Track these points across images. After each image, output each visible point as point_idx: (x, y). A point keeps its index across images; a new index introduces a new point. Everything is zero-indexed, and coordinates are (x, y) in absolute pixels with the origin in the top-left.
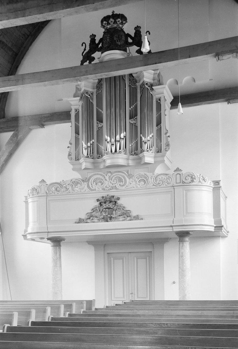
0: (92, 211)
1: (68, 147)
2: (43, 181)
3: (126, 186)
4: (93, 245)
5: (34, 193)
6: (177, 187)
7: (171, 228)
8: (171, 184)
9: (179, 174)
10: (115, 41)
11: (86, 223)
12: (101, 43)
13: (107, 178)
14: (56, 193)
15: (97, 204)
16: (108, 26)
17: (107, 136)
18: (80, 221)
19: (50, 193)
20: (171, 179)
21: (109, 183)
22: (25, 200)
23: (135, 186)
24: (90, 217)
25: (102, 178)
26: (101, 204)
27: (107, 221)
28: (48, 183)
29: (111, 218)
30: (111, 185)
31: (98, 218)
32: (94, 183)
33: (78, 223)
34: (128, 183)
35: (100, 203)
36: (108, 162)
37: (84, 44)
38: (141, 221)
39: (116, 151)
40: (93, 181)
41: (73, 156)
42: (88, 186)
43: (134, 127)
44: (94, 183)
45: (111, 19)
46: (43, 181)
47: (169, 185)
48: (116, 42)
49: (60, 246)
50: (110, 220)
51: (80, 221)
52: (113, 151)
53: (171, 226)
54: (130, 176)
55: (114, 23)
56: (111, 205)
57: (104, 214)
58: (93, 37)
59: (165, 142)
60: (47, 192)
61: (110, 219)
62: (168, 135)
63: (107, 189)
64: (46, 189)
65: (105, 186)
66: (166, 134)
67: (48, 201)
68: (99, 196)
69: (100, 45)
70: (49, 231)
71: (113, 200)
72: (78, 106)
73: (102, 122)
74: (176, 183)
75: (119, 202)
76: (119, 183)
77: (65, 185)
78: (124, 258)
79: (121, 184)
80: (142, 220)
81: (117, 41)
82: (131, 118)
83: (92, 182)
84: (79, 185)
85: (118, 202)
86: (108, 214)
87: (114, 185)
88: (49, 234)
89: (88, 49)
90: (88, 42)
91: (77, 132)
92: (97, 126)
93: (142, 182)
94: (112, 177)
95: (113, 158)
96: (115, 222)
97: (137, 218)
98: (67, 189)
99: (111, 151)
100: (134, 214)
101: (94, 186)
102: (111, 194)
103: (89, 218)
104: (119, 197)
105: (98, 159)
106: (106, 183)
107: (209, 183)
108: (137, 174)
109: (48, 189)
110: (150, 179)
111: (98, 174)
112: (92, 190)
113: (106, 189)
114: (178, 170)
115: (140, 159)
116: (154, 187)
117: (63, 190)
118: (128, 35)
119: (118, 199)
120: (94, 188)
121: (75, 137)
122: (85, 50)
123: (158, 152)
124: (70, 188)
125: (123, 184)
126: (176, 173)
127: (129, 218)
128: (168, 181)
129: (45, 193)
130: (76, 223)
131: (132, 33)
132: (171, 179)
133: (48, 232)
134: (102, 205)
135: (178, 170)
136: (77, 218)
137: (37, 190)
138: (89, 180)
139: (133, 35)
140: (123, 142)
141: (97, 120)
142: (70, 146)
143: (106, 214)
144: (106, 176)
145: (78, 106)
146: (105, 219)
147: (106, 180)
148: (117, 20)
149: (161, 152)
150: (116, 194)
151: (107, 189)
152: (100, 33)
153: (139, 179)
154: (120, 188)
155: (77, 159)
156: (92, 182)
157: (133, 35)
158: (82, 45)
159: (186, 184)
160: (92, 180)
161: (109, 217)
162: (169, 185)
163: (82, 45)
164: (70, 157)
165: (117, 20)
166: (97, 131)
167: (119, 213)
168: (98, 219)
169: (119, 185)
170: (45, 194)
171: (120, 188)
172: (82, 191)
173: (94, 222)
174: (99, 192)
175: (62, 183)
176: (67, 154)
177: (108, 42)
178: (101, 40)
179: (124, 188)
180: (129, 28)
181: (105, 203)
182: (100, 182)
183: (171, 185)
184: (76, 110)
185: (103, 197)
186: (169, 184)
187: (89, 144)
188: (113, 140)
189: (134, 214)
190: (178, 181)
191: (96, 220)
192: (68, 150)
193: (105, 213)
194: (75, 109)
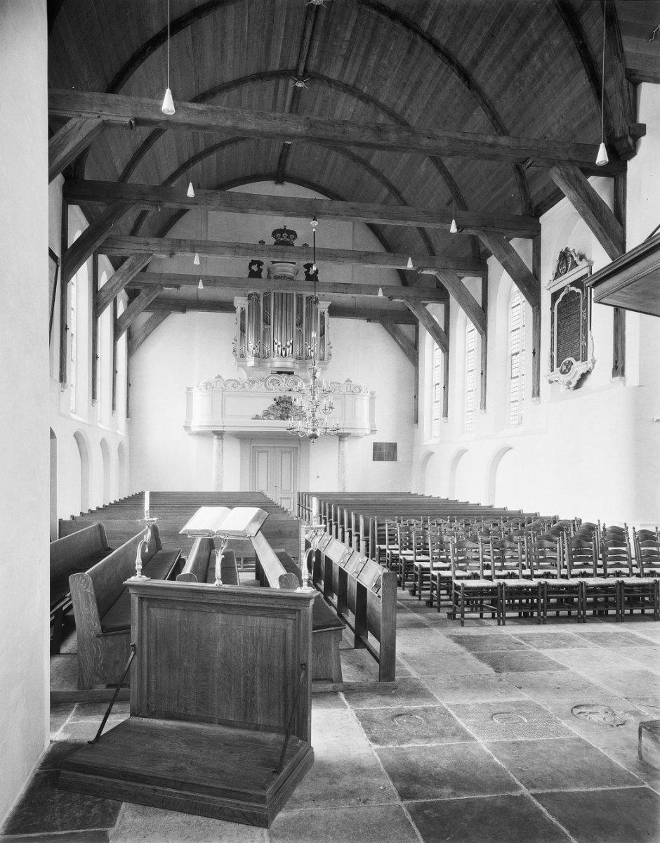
2: (219, 377)
13: (284, 380)
15: (274, 403)
18: (257, 417)
26: (278, 403)
28: (225, 378)
30: (288, 387)
39: (286, 355)
42: (265, 385)
43: (299, 332)
46: (219, 377)
49: (222, 439)
51: (257, 417)
68: (277, 396)
73: (270, 325)
82: (297, 325)
91: (243, 330)
98: (244, 387)
99: (282, 354)
102: (289, 394)
106: (283, 385)
107: (368, 394)
112: (270, 390)
114: (348, 381)
123: (321, 360)
124: (247, 385)
135: (348, 381)
136: (254, 415)
141: (264, 321)
146: (282, 418)
160: (269, 380)
166: (264, 332)
175: (239, 381)
181: (282, 402)
185: (280, 397)
191: (272, 417)
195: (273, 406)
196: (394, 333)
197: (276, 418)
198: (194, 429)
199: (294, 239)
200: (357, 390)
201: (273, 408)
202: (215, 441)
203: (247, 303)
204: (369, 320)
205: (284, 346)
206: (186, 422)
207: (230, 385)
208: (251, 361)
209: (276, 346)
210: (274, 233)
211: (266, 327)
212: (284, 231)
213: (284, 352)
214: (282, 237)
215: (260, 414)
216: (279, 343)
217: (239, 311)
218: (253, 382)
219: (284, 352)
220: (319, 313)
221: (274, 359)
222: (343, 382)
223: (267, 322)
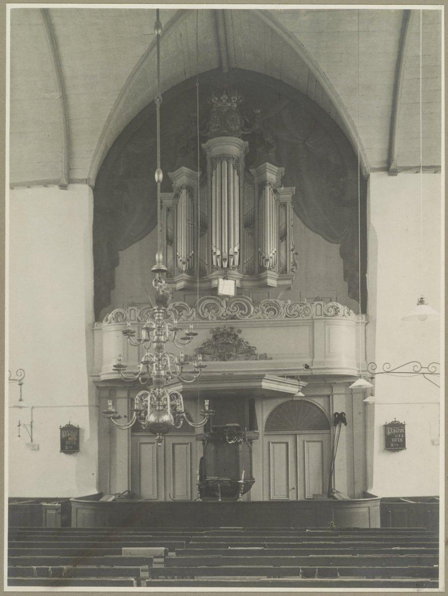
0: (203, 346)
3: (250, 315)
5: (119, 320)
6: (317, 321)
9: (319, 304)
17: (216, 247)
19: (143, 320)
20: (308, 310)
21: (227, 311)
25: (218, 304)
26: (215, 337)
30: (229, 313)
31: (211, 356)
32: (207, 310)
34: (252, 312)
40: (204, 306)
42: (198, 314)
44: (207, 310)
47: (307, 318)
54: (256, 303)
57: (220, 351)
60: (140, 318)
63: (225, 318)
64: (137, 315)
65: (221, 314)
74: (317, 315)
76: (241, 311)
79: (243, 312)
83: (203, 309)
84: (184, 312)
87: (234, 314)
104: (240, 329)
108: (263, 301)
110: (282, 308)
112: (203, 319)
113: (222, 318)
119: (240, 331)
120: (206, 315)
123: (282, 273)
124: (173, 316)
125: (245, 313)
128: (306, 312)
129: (136, 320)
132: (308, 310)
137: (125, 315)
140: (237, 257)
143: (223, 351)
147: (222, 306)
149: (286, 273)
151: (225, 318)
153: (268, 308)
156: (203, 309)
159: (327, 318)
161: (227, 355)
162: (307, 318)
172: (192, 318)
179: (247, 318)
182: (214, 309)
184: (169, 209)
187: (188, 256)
188: (225, 255)
189: (259, 352)
190: (319, 313)
193: (222, 350)
200: (333, 313)
205: (225, 255)
209: (214, 257)
213: (225, 265)
219: (225, 265)
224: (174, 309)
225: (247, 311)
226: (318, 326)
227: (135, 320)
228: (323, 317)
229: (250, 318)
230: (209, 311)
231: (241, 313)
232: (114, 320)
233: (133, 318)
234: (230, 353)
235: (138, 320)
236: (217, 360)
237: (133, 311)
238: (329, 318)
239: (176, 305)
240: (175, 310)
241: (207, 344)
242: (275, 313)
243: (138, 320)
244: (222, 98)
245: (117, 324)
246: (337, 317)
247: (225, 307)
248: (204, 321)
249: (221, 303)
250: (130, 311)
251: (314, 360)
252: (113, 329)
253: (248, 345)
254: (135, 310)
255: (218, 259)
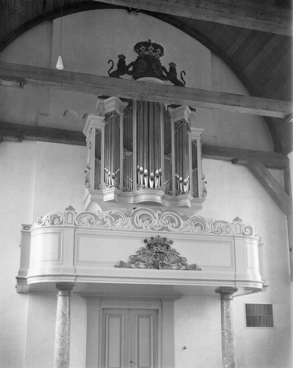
0: (137, 254)
1: (86, 172)
2: (71, 208)
4: (85, 298)
5: (55, 222)
7: (234, 283)
8: (231, 234)
10: (154, 69)
11: (130, 268)
12: (131, 67)
13: (156, 215)
14: (89, 226)
15: (144, 245)
16: (146, 53)
18: (122, 265)
19: (80, 224)
22: (21, 230)
23: (190, 230)
24: (135, 261)
25: (149, 214)
26: (149, 246)
27: (158, 268)
29: (163, 265)
32: (141, 219)
33: (118, 267)
34: (182, 225)
35: (149, 245)
36: (143, 198)
37: (111, 62)
38: (199, 272)
41: (92, 182)
42: (133, 222)
43: (168, 164)
45: (151, 47)
46: (71, 208)
48: (154, 71)
50: (162, 267)
51: (122, 265)
52: (151, 185)
53: (235, 281)
55: (153, 51)
56: (163, 250)
57: (154, 259)
58: (122, 59)
59: (202, 187)
60: (77, 223)
61: (162, 266)
62: (204, 181)
63: (158, 229)
64: (74, 218)
65: (154, 225)
66: (203, 179)
67: (76, 234)
68: (148, 236)
69: (131, 69)
70: (79, 274)
71: (165, 243)
72: (101, 127)
73: (131, 150)
75: (172, 247)
77: (101, 218)
78: (123, 317)
79: (174, 225)
80: (201, 270)
81: (156, 71)
82: (165, 154)
85: (171, 245)
86: (160, 260)
87: (166, 226)
88: (78, 278)
89: (115, 68)
90: (116, 61)
91: (98, 156)
92: (124, 154)
93: (199, 227)
94: (163, 216)
95: (152, 194)
96: (166, 271)
97: (194, 267)
98: (104, 223)
100: (190, 262)
101: (140, 224)
102: (163, 235)
103: (134, 263)
104: (172, 240)
105: (124, 191)
106: (155, 222)
109: (77, 219)
111: (145, 210)
113: (155, 228)
114: (237, 219)
115: (177, 200)
116: (212, 234)
117: (98, 223)
118: (164, 69)
119: (171, 242)
120: (140, 224)
121: (96, 161)
122: (112, 68)
124: (109, 222)
126: (236, 222)
127: (184, 267)
128: (228, 229)
129: (73, 224)
130: (116, 266)
131: (168, 69)
133: (77, 276)
134: (152, 248)
136: (117, 260)
137: (61, 219)
138: (133, 214)
139: (168, 70)
141: (125, 147)
142: (88, 170)
144: (155, 213)
145: (101, 127)
146: (156, 266)
147: (155, 218)
148: (157, 50)
149: (198, 197)
150: (169, 237)
152: (131, 57)
153: (195, 224)
154: (173, 229)
155: (97, 186)
157: (168, 70)
158: (109, 62)
160: (137, 215)
162: (228, 235)
163: (109, 62)
164: (87, 183)
165: (157, 50)
166: (124, 160)
167: (172, 259)
168: (146, 265)
169: (171, 225)
170: (73, 225)
171: (173, 229)
172: (127, 226)
173: (140, 268)
174: (146, 231)
176: (85, 180)
177: (145, 68)
178: (132, 64)
179: (177, 230)
180: (164, 61)
181: (156, 245)
182: (149, 219)
183: (231, 234)
185: (152, 238)
186: (228, 233)
189: (190, 262)
190: (238, 232)
191: (142, 265)
192: (85, 175)
193: (156, 258)
194: (96, 129)
195: (143, 249)
196: (261, 179)
197: (147, 267)
198: (30, 281)
199: (161, 55)
201: (142, 252)
202: (60, 299)
203: (104, 124)
204: (234, 162)
205: (152, 174)
206: (20, 272)
207: (85, 220)
208: (109, 195)
209: (141, 177)
210: (137, 47)
211: (128, 154)
212: (147, 44)
214: (147, 50)
215: (126, 260)
216: (146, 171)
217: (91, 139)
218: (117, 217)
220: (190, 141)
221: (138, 192)
222: (230, 220)
223: (128, 147)
224: (110, 216)
225: (177, 223)
226: (238, 241)
227: (72, 224)
228: (241, 235)
229: (181, 231)
230: (143, 221)
231: (172, 226)
232: (49, 222)
233: (69, 222)
234: (164, 262)
235: (75, 224)
236: (151, 268)
237: (70, 215)
238: (247, 236)
239: (112, 213)
240: (111, 218)
241: (141, 252)
242: (202, 228)
243: (75, 224)
244: (149, 48)
245: (53, 226)
246: (252, 236)
247: (158, 219)
248: (138, 230)
249: (154, 215)
250: (67, 214)
251: (237, 273)
252: (41, 232)
253: (179, 256)
254: (72, 214)
255: (145, 178)
